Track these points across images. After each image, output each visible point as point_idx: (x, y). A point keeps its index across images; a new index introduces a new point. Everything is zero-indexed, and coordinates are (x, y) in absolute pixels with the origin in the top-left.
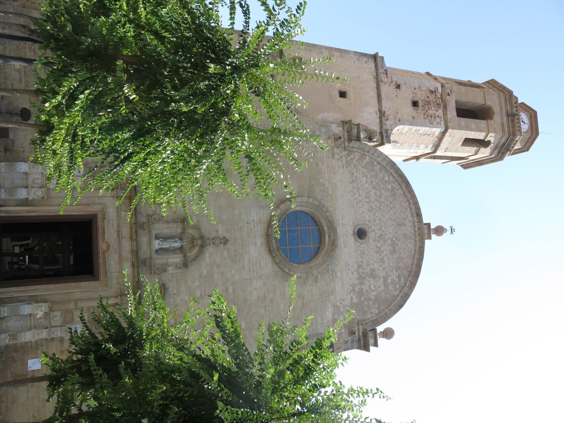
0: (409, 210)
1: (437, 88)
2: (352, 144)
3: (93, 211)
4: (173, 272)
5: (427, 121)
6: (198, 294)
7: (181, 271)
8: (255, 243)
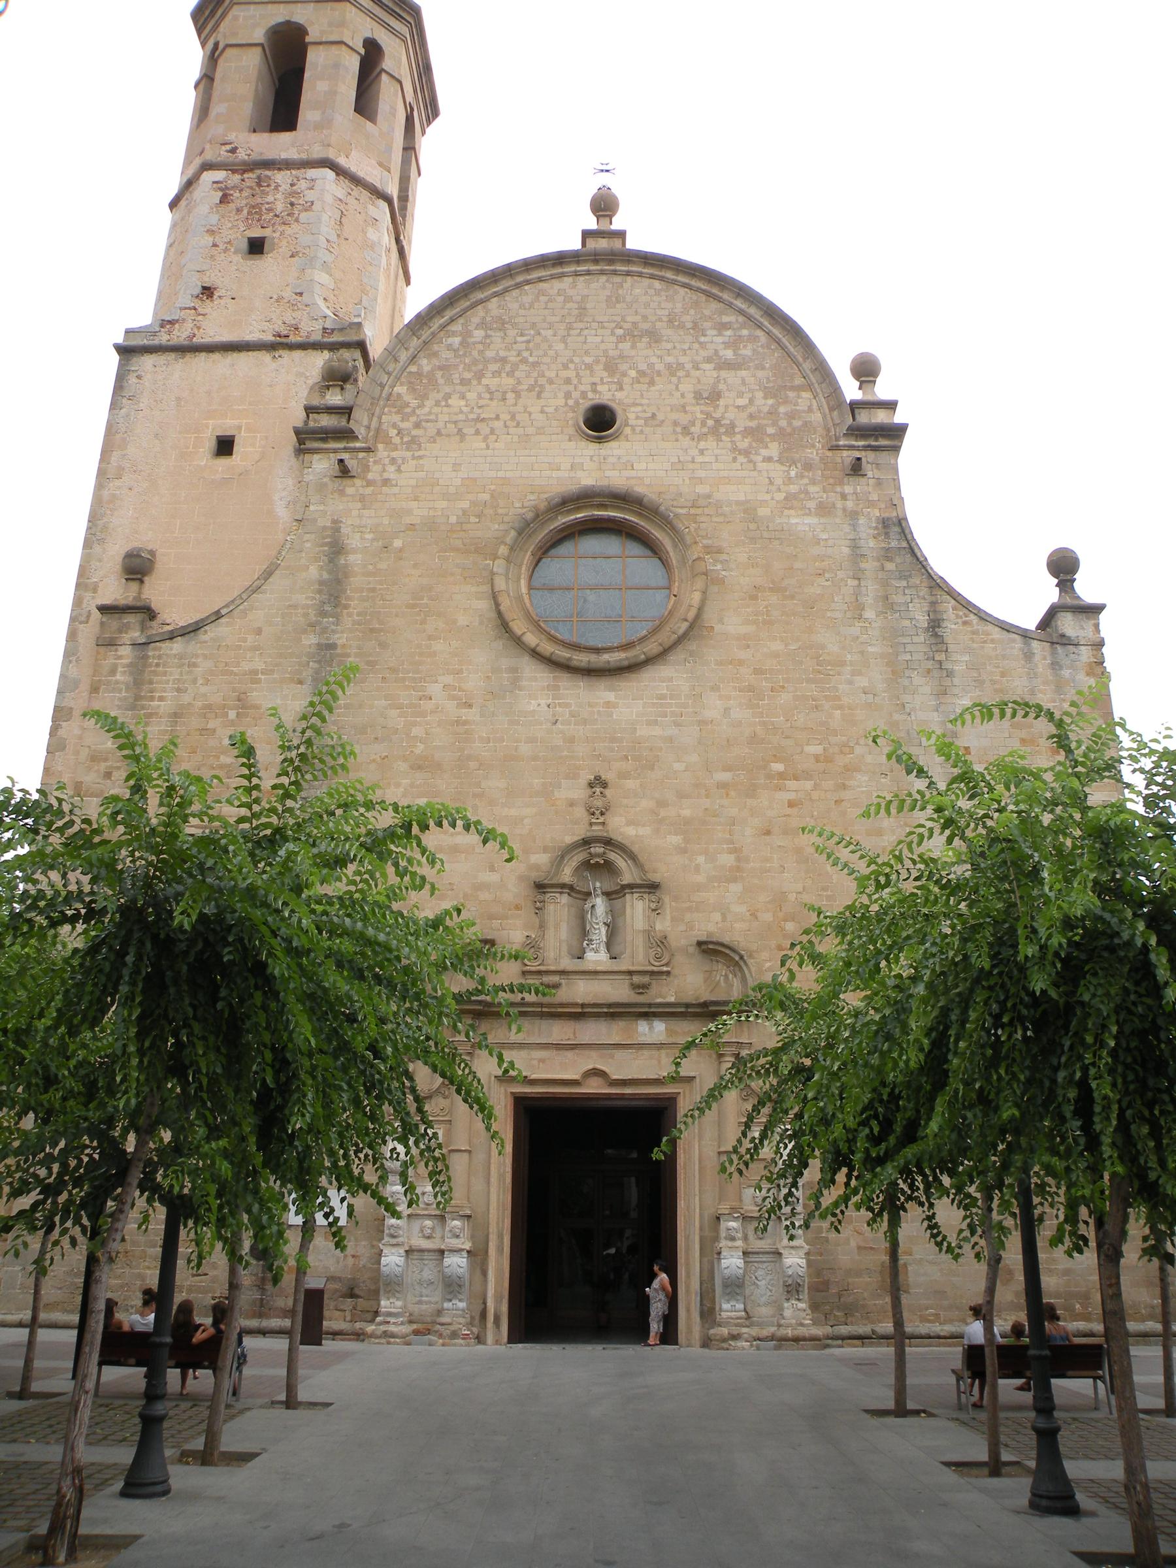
0: (542, 285)
2: (360, 431)
4: (668, 917)
5: (304, 217)
6: (727, 860)
7: (667, 899)
8: (608, 704)
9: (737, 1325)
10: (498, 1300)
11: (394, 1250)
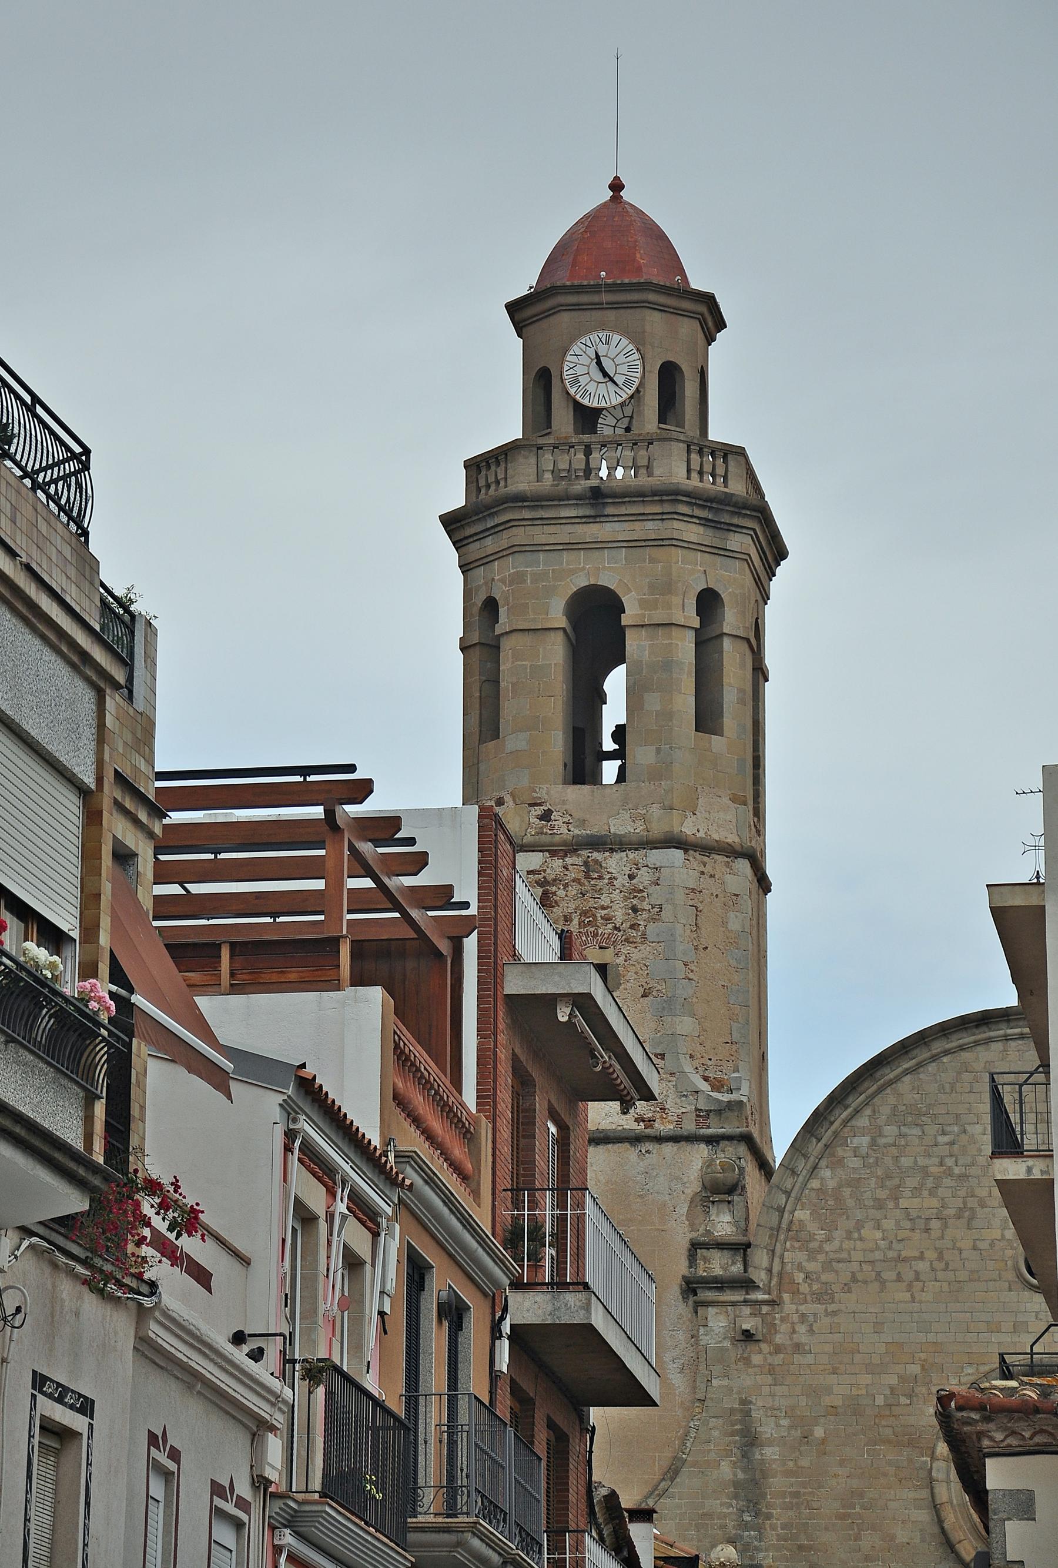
0: (965, 1055)
1: (529, 872)
2: (759, 1277)
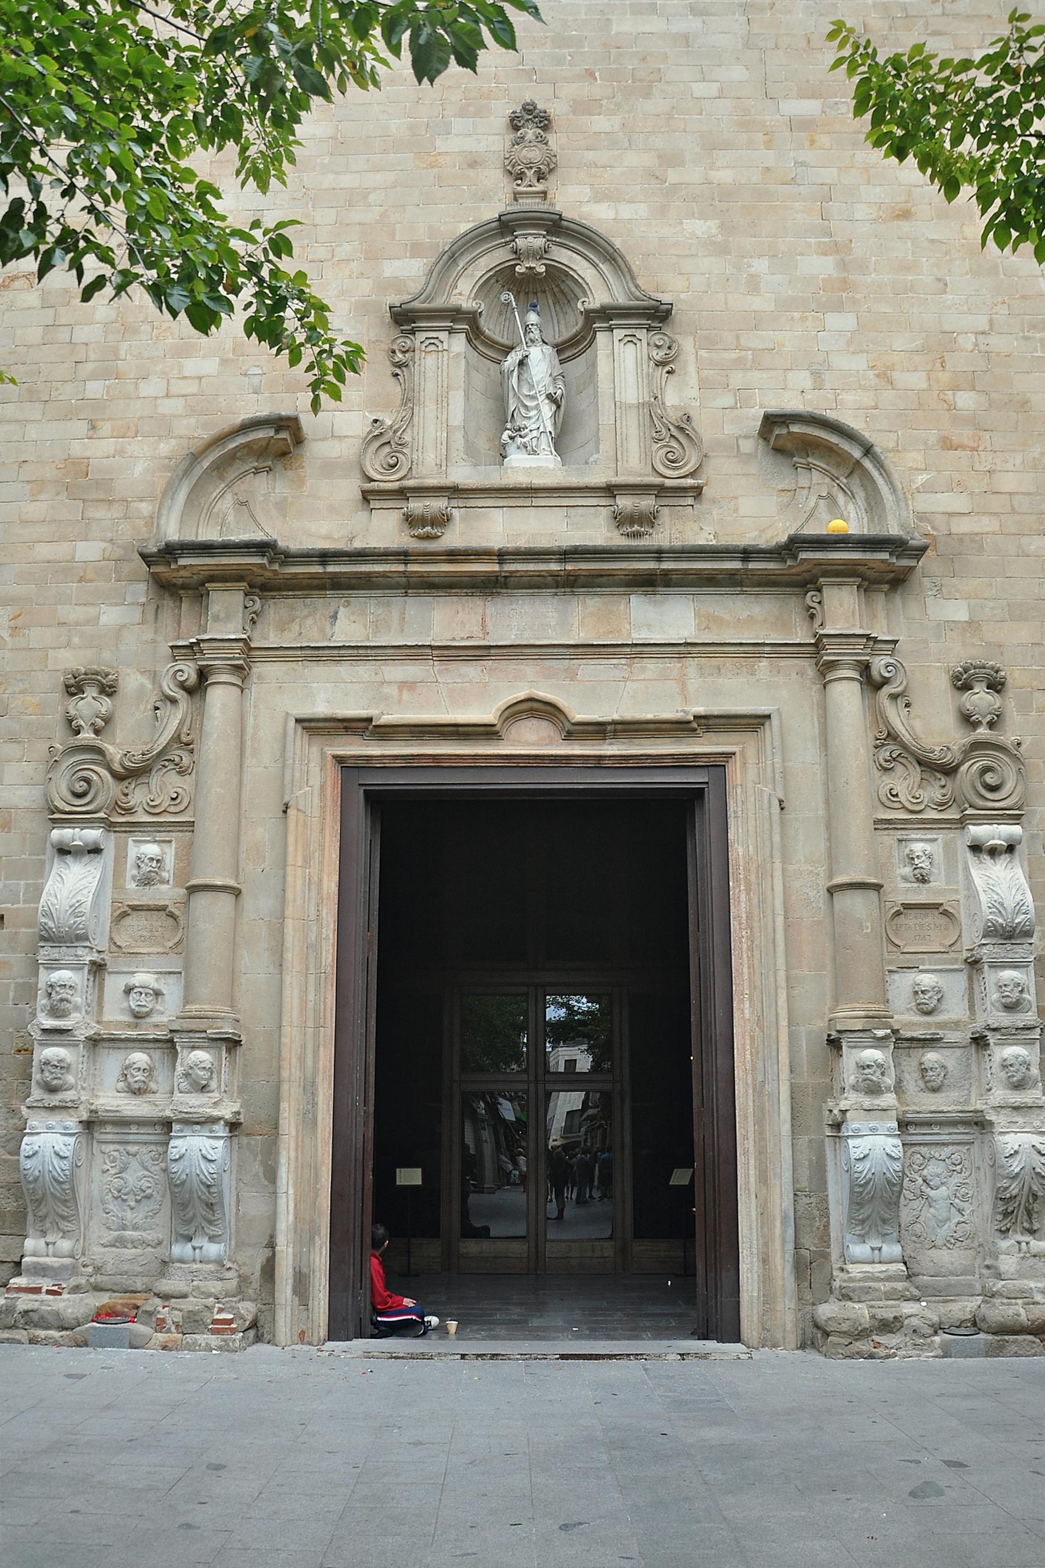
3: (323, 787)
4: (693, 380)
6: (823, 266)
7: (687, 344)
9: (889, 1296)
10: (304, 1237)
11: (53, 1120)
